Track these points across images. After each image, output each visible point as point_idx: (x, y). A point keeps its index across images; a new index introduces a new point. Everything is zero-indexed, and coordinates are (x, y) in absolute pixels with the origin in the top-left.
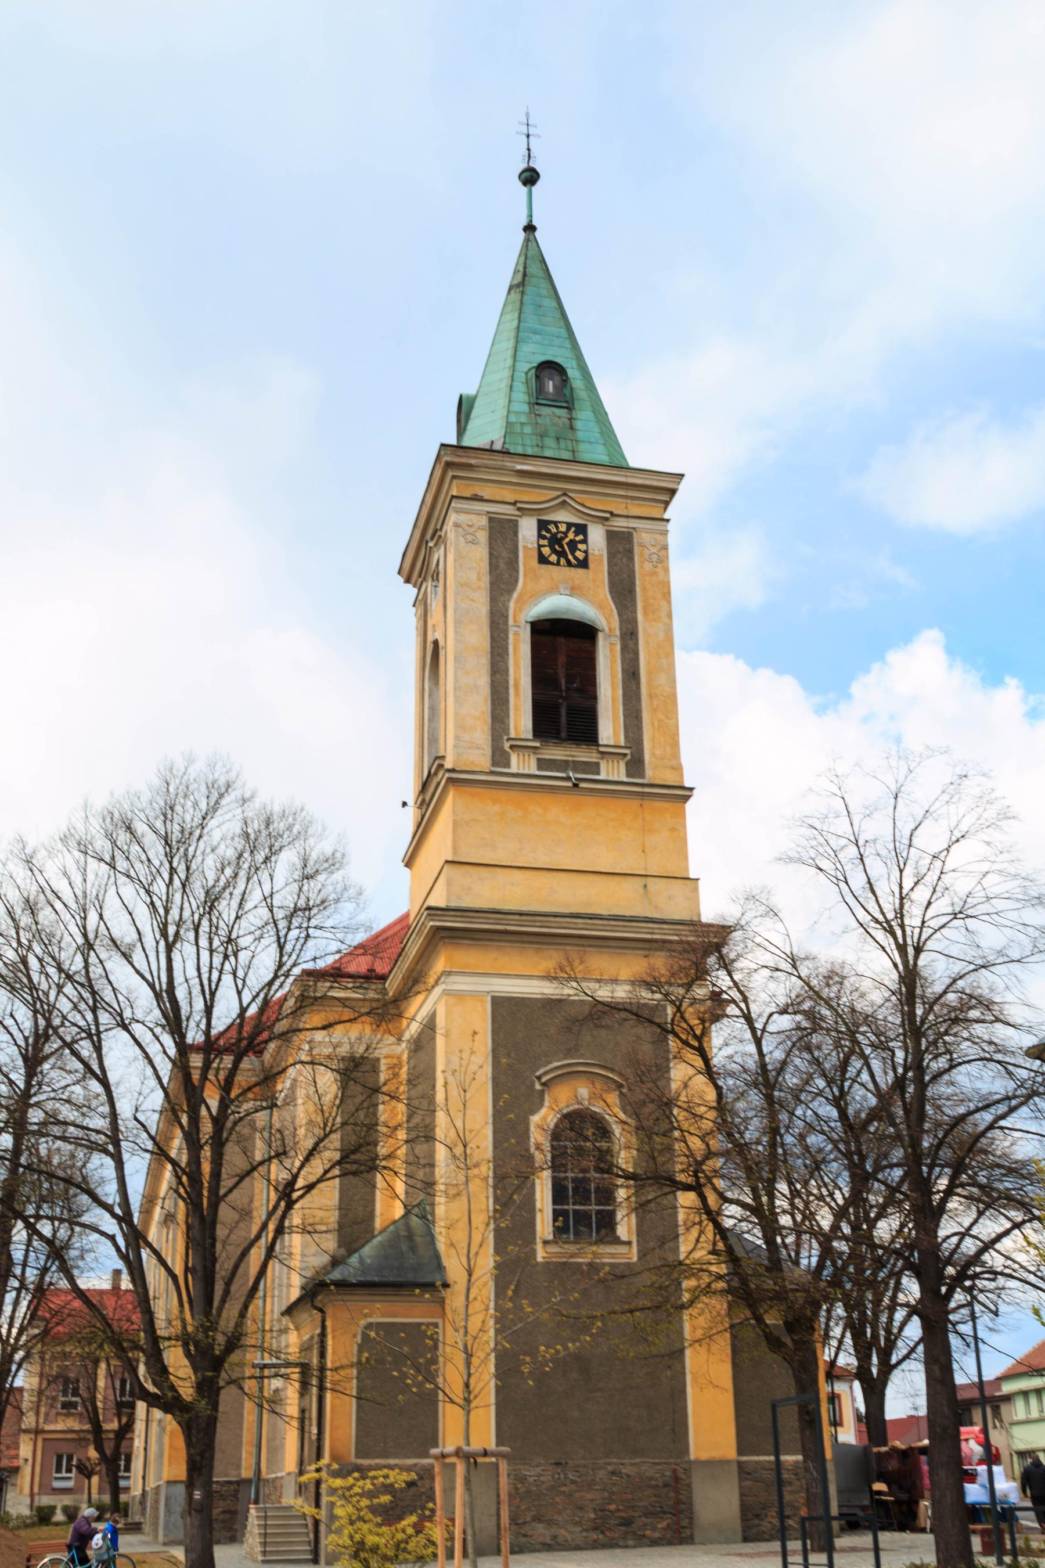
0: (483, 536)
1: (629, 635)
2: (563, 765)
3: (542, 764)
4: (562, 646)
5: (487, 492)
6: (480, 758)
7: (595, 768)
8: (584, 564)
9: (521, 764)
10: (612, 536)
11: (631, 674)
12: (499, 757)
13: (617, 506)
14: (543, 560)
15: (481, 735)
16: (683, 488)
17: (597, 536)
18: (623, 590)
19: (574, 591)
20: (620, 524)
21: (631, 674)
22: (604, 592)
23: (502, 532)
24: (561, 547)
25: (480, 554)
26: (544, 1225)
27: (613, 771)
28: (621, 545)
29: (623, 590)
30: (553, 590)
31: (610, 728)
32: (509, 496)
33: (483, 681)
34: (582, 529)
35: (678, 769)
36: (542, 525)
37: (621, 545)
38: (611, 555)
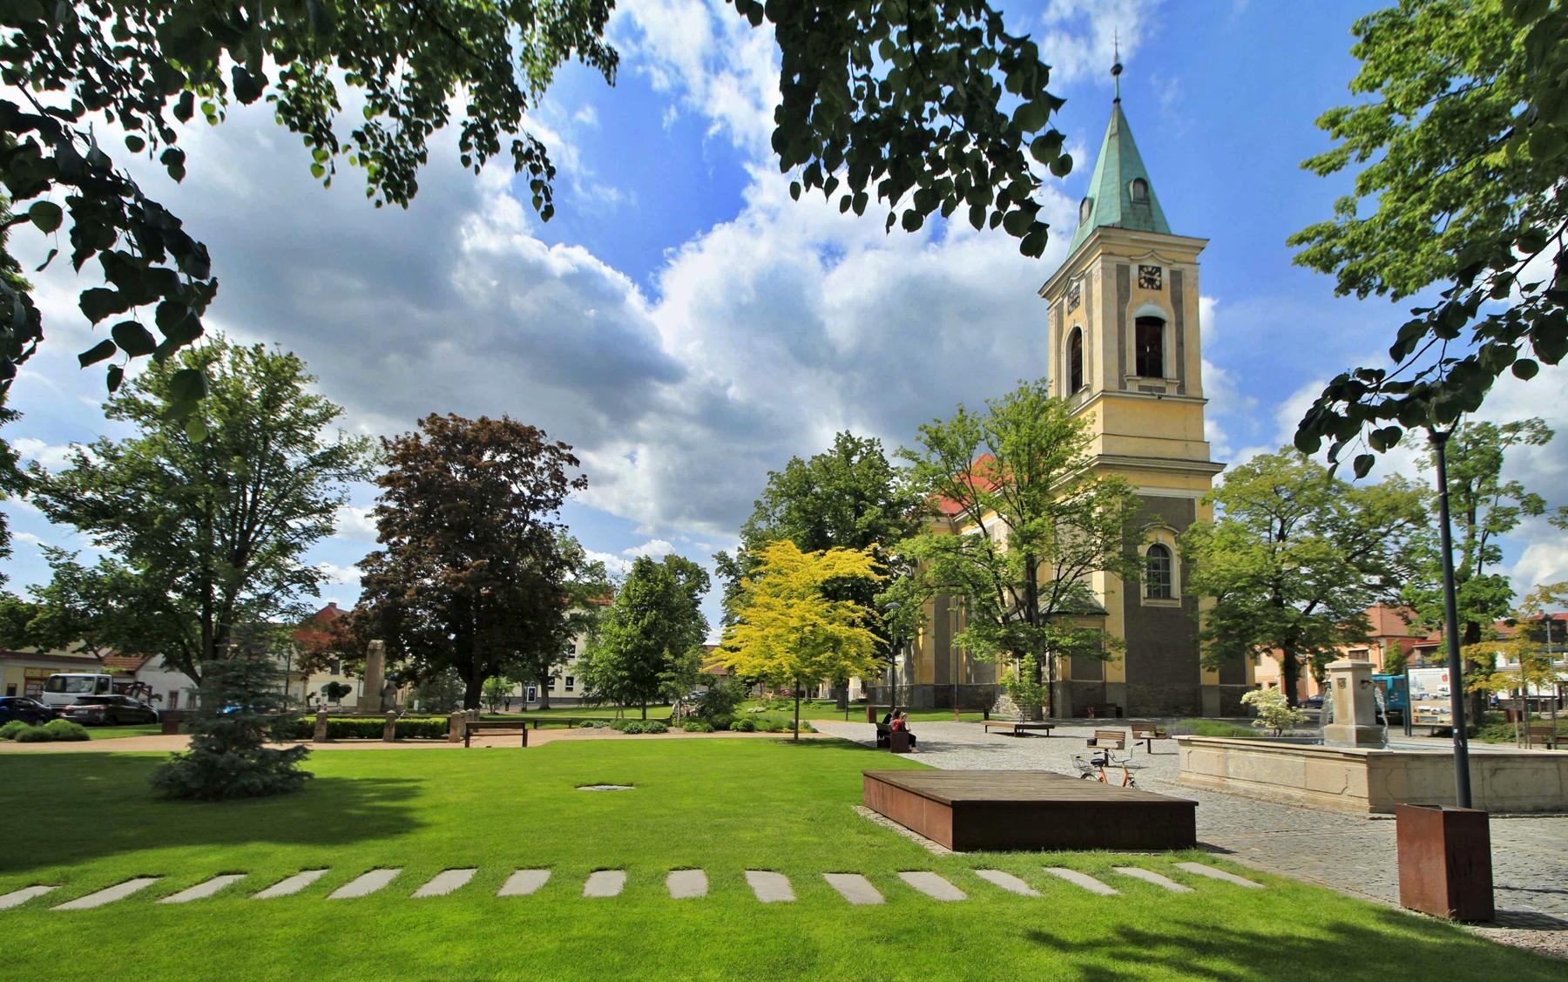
0: (1114, 274)
1: (1180, 324)
2: (1150, 389)
3: (1141, 388)
4: (1150, 328)
5: (1116, 250)
6: (1115, 386)
7: (1163, 390)
8: (1159, 288)
9: (1132, 387)
10: (1172, 273)
11: (1180, 344)
12: (1122, 385)
13: (1174, 256)
14: (1141, 286)
15: (1115, 374)
16: (1208, 246)
17: (1165, 273)
18: (1177, 301)
19: (1156, 302)
20: (1176, 267)
21: (1180, 344)
22: (1168, 303)
23: (1123, 271)
24: (1150, 279)
25: (1113, 283)
26: (1144, 591)
27: (1172, 391)
28: (1176, 276)
29: (1177, 301)
30: (1147, 301)
31: (1170, 369)
32: (1127, 252)
33: (1116, 347)
34: (1159, 269)
35: (1201, 390)
36: (1141, 268)
37: (1176, 276)
38: (1172, 282)
